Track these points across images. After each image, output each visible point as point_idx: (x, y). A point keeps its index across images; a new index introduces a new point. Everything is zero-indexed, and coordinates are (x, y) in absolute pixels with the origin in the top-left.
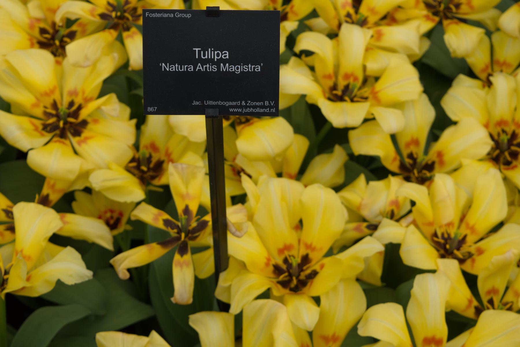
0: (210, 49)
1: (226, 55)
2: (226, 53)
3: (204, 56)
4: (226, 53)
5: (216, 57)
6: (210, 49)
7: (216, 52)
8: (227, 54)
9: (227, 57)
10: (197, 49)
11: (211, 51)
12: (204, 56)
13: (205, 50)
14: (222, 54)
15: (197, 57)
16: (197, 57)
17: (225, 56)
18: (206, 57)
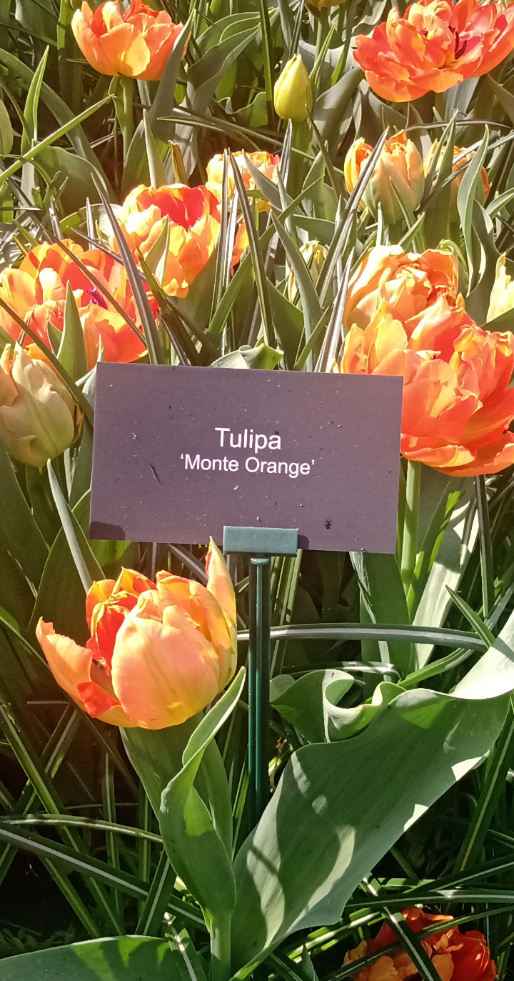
0: (246, 431)
1: (276, 443)
2: (277, 439)
3: (236, 442)
4: (277, 439)
5: (257, 446)
6: (246, 431)
7: (257, 437)
8: (279, 442)
9: (279, 447)
10: (222, 430)
11: (249, 433)
12: (236, 442)
13: (237, 430)
14: (269, 441)
15: (222, 445)
16: (222, 445)
17: (273, 445)
18: (239, 445)
